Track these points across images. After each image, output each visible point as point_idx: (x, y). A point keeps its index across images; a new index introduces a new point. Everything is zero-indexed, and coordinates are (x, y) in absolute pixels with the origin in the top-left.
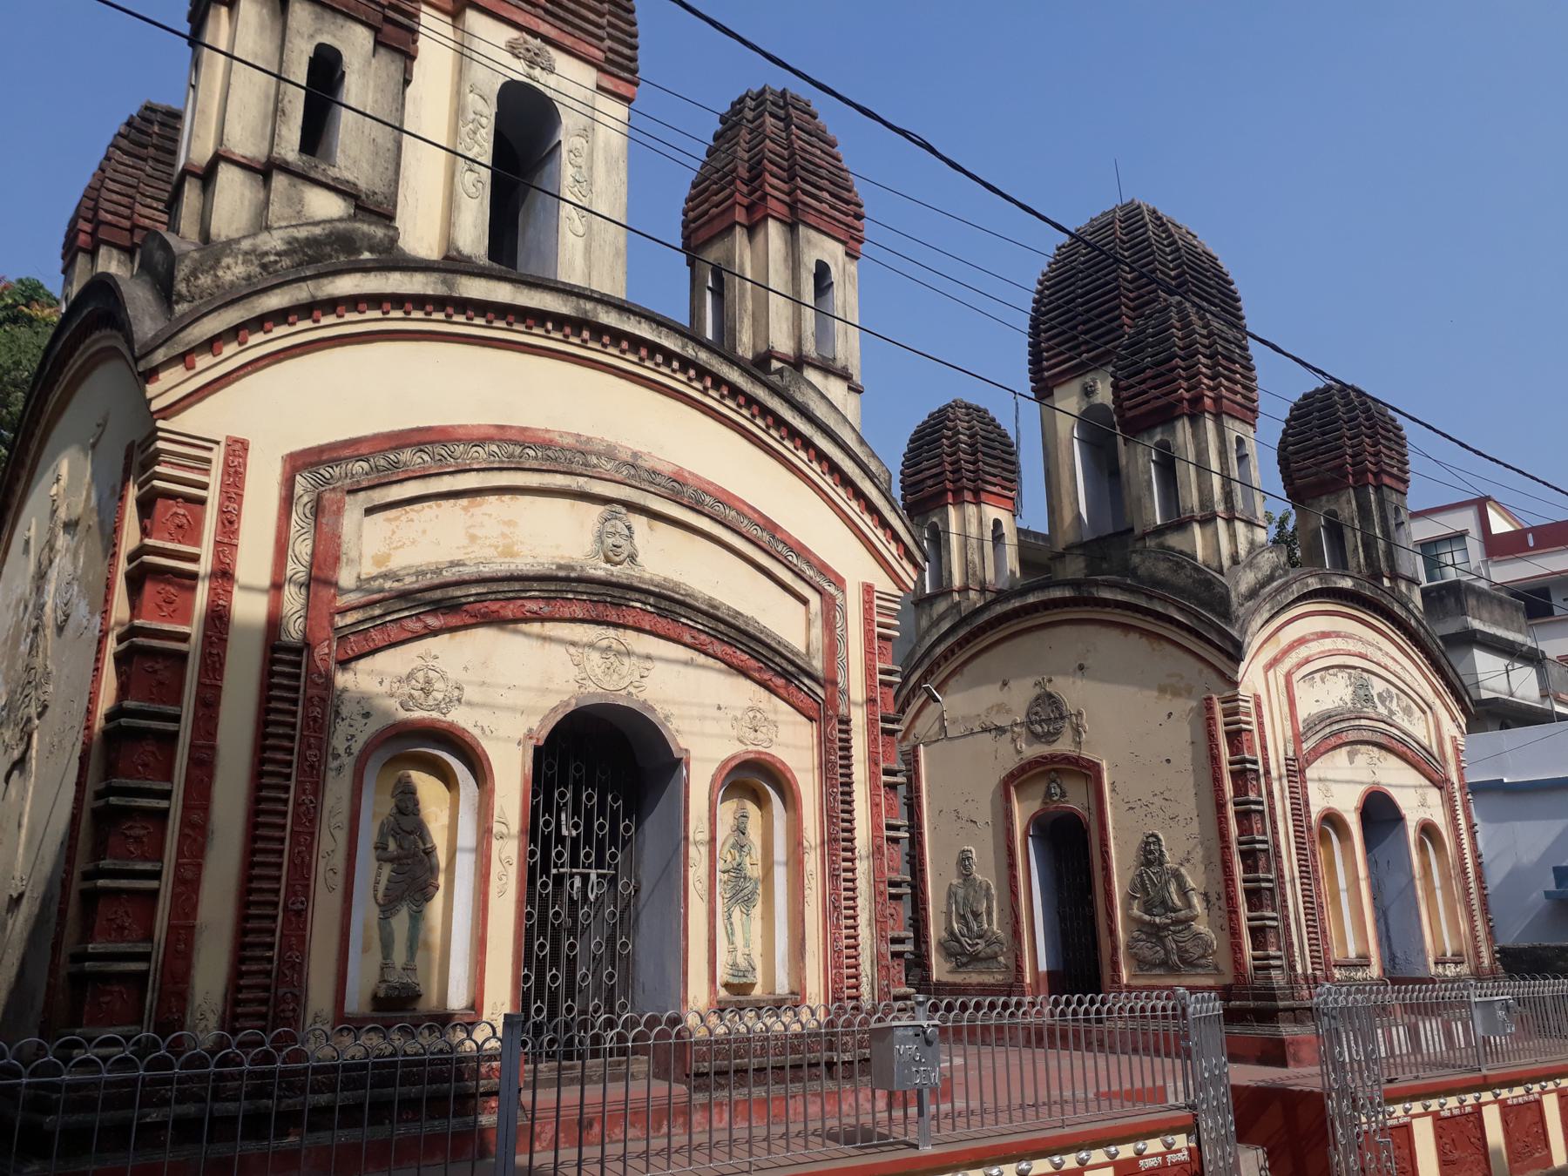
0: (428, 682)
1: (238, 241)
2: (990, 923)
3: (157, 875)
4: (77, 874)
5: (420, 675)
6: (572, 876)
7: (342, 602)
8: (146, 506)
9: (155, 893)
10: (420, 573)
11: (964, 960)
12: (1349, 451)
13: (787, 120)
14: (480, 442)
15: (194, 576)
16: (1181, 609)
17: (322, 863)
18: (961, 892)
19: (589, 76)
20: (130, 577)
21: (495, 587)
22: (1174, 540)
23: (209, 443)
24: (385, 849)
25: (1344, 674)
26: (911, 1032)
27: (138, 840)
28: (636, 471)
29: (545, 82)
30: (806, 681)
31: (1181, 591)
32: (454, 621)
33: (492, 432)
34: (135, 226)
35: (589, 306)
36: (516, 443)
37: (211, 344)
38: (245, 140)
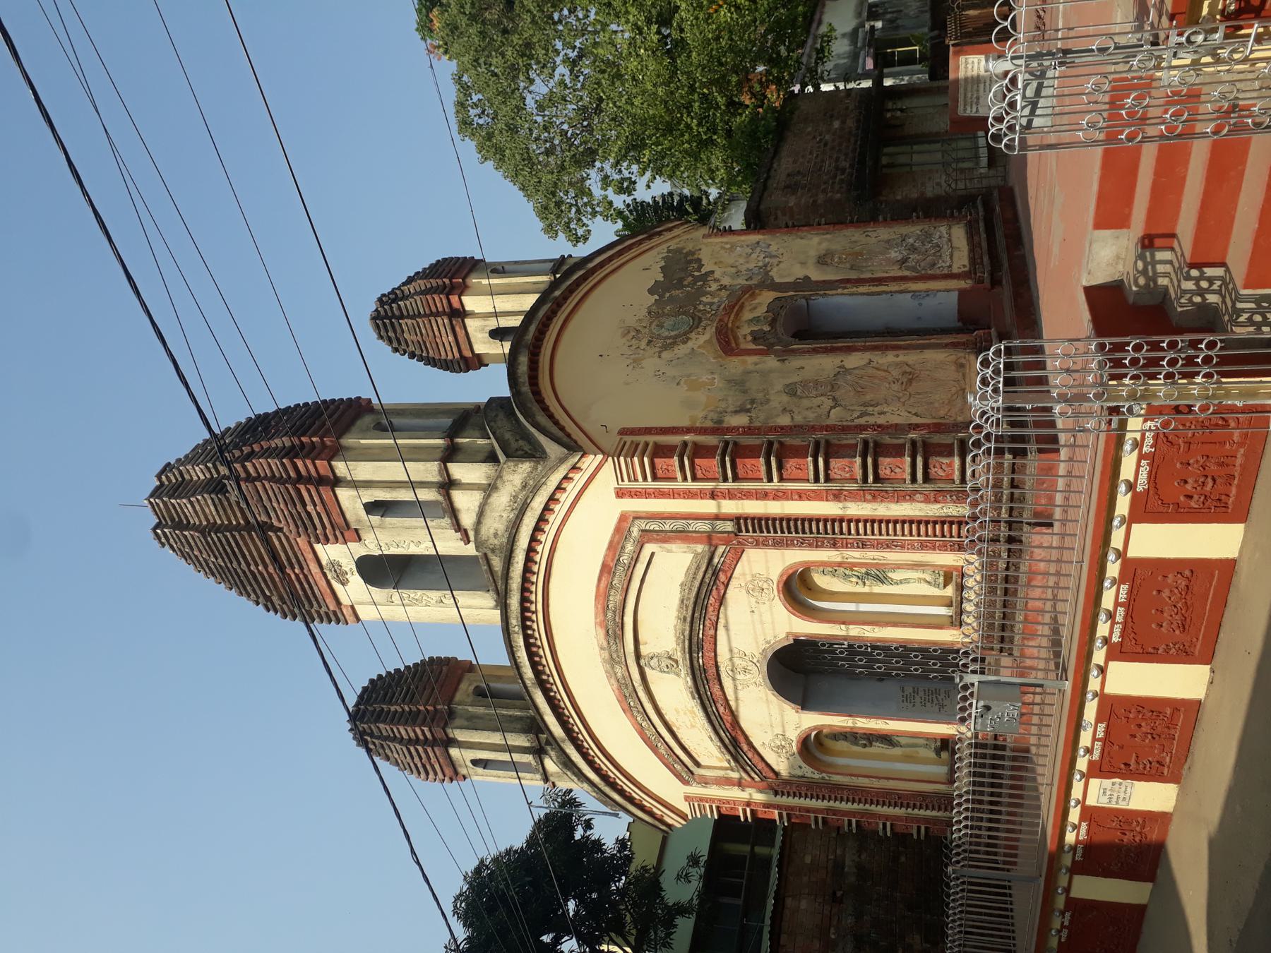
21: (718, 727)
26: (979, 720)
29: (349, 565)
32: (741, 739)
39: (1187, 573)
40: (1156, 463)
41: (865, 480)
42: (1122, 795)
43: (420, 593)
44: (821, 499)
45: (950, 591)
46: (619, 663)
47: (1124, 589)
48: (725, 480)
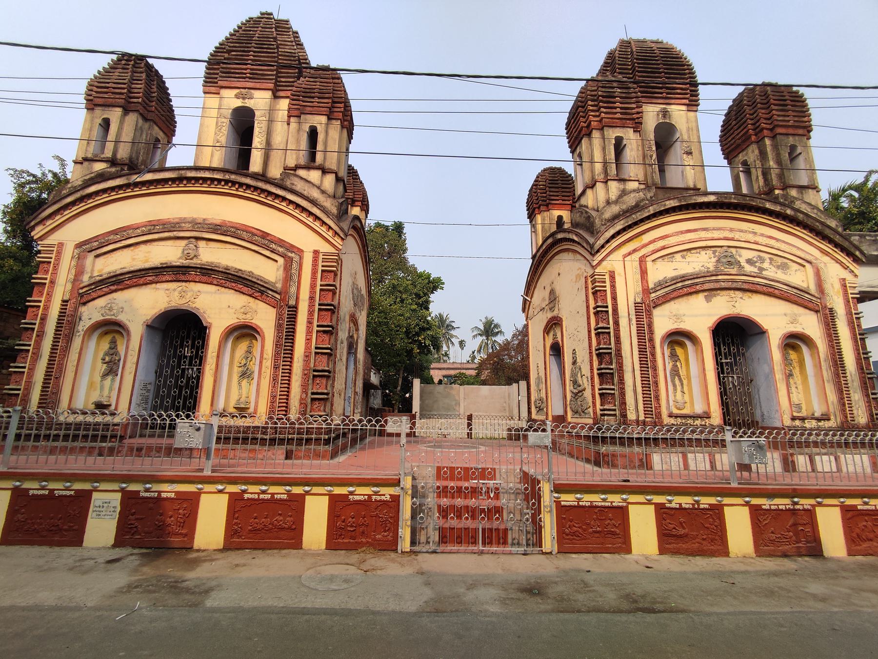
12: (750, 122)
28: (196, 225)
29: (249, 103)
30: (270, 292)
35: (183, 172)
39: (294, 527)
40: (367, 503)
41: (315, 371)
42: (102, 514)
43: (226, 133)
44: (306, 349)
45: (232, 410)
46: (193, 227)
47: (285, 497)
48: (320, 305)
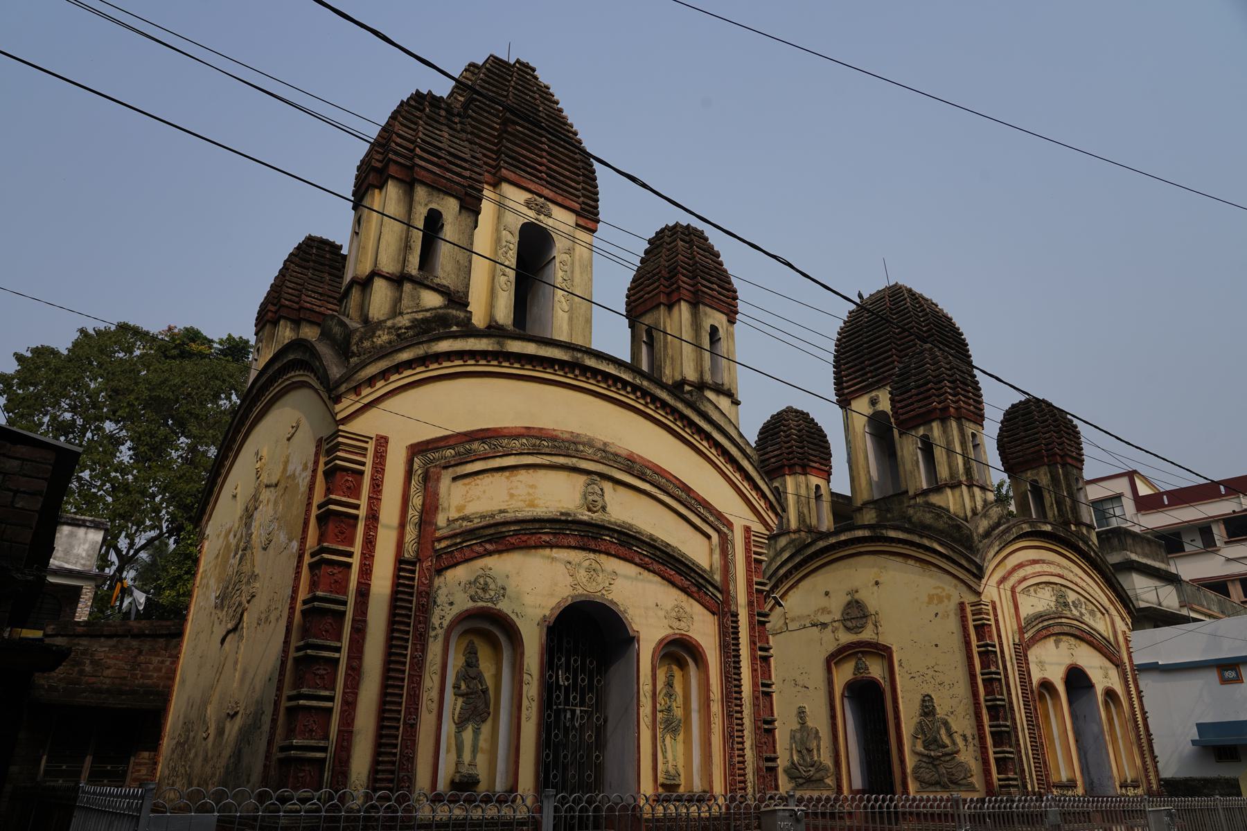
0: (486, 584)
1: (385, 321)
2: (819, 755)
3: (331, 699)
4: (284, 697)
5: (482, 581)
6: (565, 711)
7: (438, 534)
8: (328, 474)
9: (330, 710)
10: (483, 517)
11: (801, 781)
13: (690, 242)
14: (517, 436)
15: (356, 517)
16: (941, 544)
17: (425, 695)
18: (798, 735)
19: (570, 218)
20: (318, 518)
22: (935, 499)
23: (366, 439)
24: (459, 688)
25: (1048, 589)
26: (787, 814)
27: (322, 677)
28: (607, 455)
31: (941, 532)
33: (523, 431)
34: (301, 308)
35: (579, 355)
36: (537, 438)
37: (371, 381)
38: (388, 264)
